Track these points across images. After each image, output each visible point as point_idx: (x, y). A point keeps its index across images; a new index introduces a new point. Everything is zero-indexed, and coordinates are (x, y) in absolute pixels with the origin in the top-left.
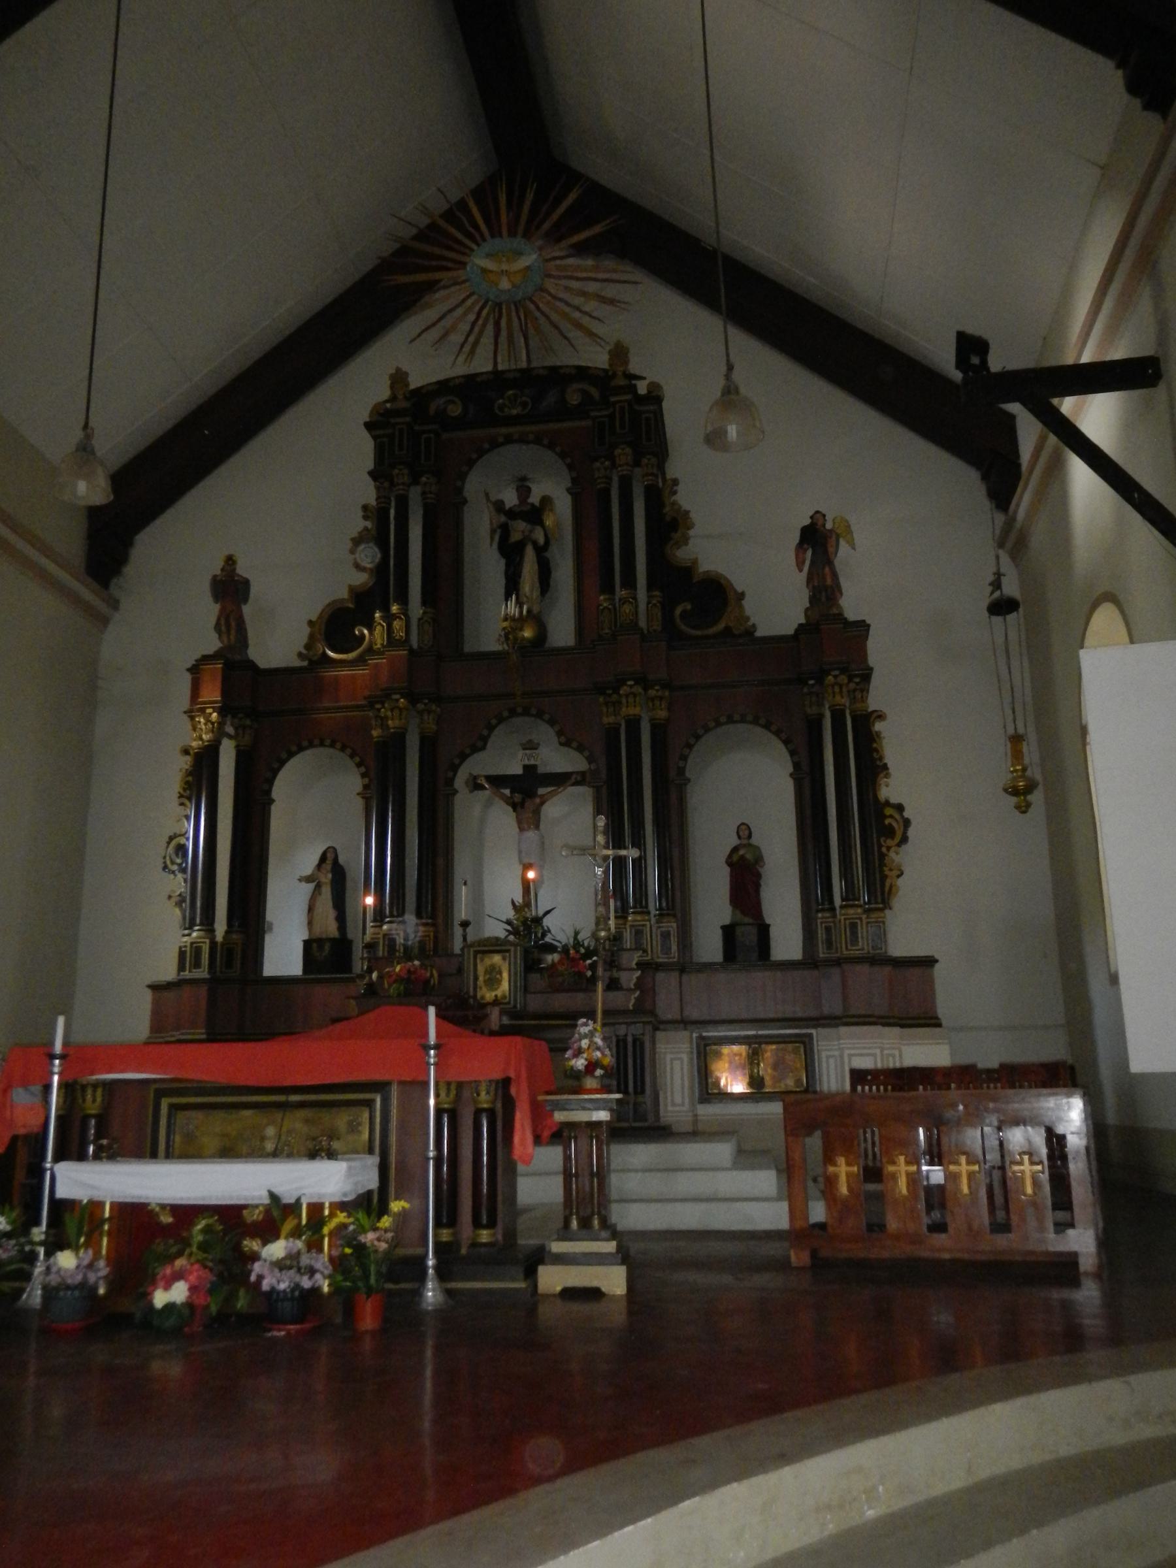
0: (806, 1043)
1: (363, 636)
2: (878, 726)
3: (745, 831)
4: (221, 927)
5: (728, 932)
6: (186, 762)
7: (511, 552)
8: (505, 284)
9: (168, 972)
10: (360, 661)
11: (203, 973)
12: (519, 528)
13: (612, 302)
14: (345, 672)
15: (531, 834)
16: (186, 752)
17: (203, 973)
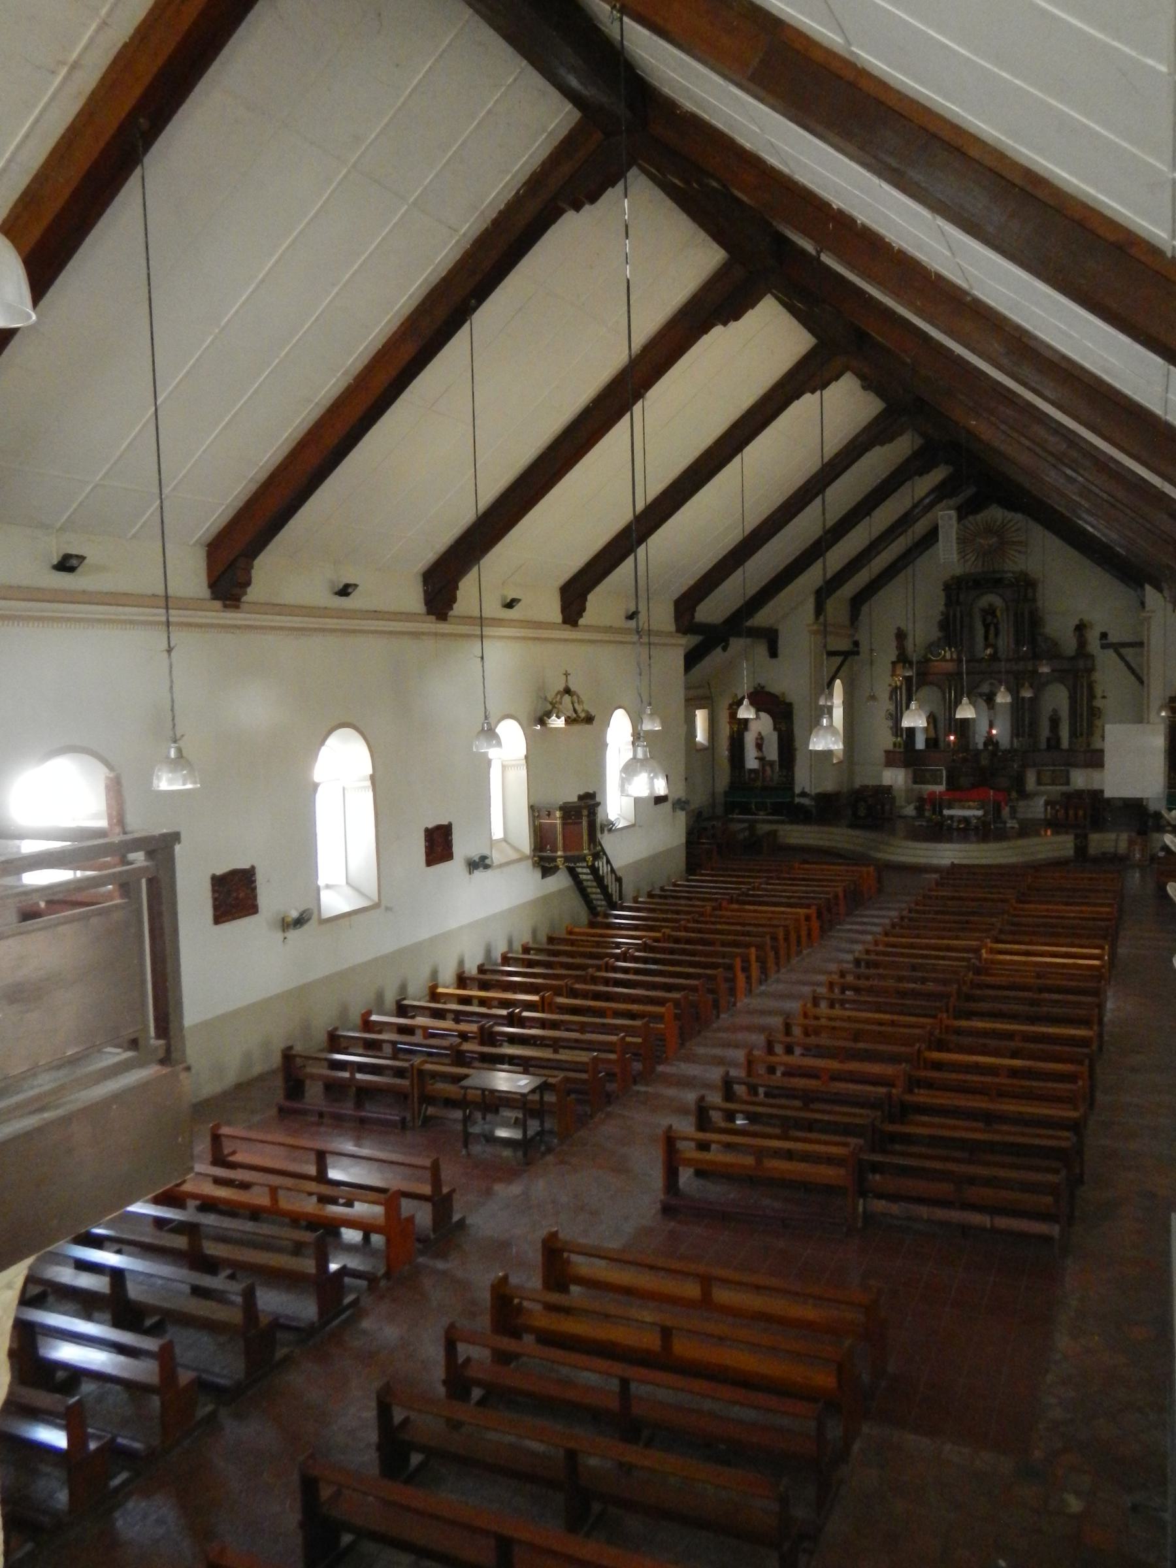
0: (1068, 772)
1: (940, 654)
2: (1095, 684)
3: (1055, 711)
4: (904, 736)
5: (1048, 740)
6: (889, 689)
7: (987, 627)
8: (986, 547)
9: (890, 747)
10: (941, 660)
11: (902, 750)
12: (989, 619)
13: (1020, 552)
14: (936, 663)
15: (992, 711)
16: (890, 685)
17: (902, 750)
